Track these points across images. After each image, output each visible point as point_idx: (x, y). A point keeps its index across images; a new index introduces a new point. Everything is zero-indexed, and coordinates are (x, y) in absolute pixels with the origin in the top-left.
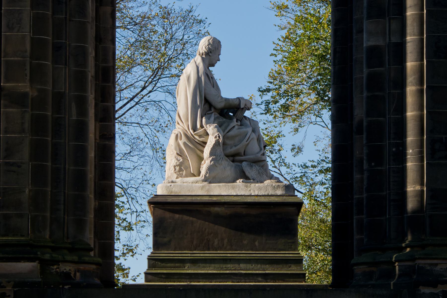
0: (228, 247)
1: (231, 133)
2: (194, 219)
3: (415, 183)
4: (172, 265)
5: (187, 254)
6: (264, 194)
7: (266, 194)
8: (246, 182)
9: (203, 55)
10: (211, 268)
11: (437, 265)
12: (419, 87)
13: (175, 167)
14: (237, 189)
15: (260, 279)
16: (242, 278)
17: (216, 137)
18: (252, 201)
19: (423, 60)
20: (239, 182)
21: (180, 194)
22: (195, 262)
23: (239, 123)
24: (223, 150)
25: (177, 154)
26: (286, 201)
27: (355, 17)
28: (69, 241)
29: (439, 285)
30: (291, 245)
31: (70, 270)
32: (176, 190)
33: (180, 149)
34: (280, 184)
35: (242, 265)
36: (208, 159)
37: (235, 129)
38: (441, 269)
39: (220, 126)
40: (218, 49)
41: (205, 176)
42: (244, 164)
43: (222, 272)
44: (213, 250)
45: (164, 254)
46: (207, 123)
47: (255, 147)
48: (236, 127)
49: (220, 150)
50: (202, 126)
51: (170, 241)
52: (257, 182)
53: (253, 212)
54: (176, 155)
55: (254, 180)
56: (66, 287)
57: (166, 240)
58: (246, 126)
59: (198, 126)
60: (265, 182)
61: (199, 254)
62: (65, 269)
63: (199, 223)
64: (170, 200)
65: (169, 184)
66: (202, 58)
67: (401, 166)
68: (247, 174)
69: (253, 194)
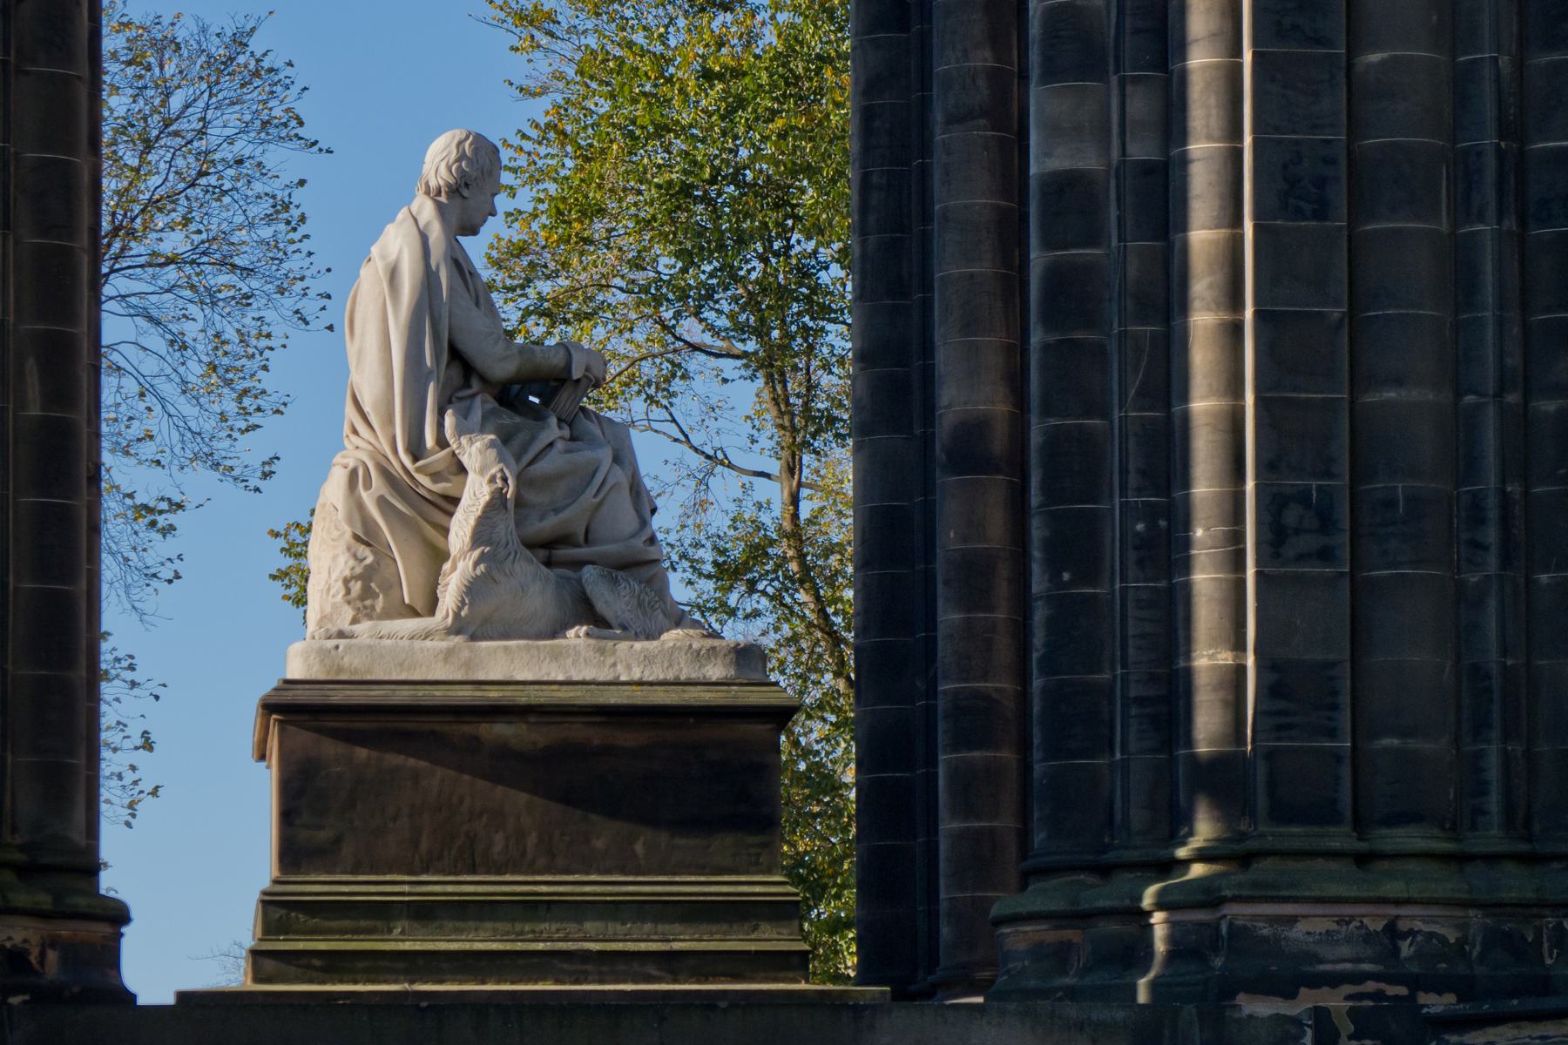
0: (542, 862)
1: (544, 466)
2: (423, 764)
3: (1214, 643)
5: (398, 886)
6: (661, 677)
7: (670, 676)
8: (599, 637)
9: (439, 193)
10: (482, 935)
11: (1292, 920)
12: (1226, 316)
13: (346, 581)
14: (569, 661)
15: (655, 973)
16: (589, 967)
17: (492, 480)
18: (625, 701)
19: (1237, 221)
21: (369, 677)
22: (424, 913)
24: (518, 524)
25: (357, 538)
26: (740, 702)
27: (939, 69)
28: (18, 841)
29: (1303, 990)
30: (759, 855)
31: (25, 941)
32: (354, 664)
33: (367, 522)
34: (716, 643)
35: (590, 927)
36: (463, 555)
37: (554, 452)
38: (1309, 933)
39: (506, 438)
40: (490, 173)
41: (457, 615)
42: (589, 573)
43: (519, 946)
44: (488, 873)
45: (318, 885)
46: (460, 431)
48: (560, 445)
49: (505, 526)
50: (442, 443)
51: (337, 841)
52: (637, 637)
53: (628, 738)
54: (353, 541)
55: (624, 628)
56: (15, 1000)
57: (324, 835)
58: (593, 443)
59: (430, 440)
60: (665, 636)
61: (439, 886)
62: (10, 938)
63: (438, 778)
64: (338, 696)
65: (331, 643)
66: (440, 207)
67: (1163, 584)
68: (600, 606)
69: (623, 678)
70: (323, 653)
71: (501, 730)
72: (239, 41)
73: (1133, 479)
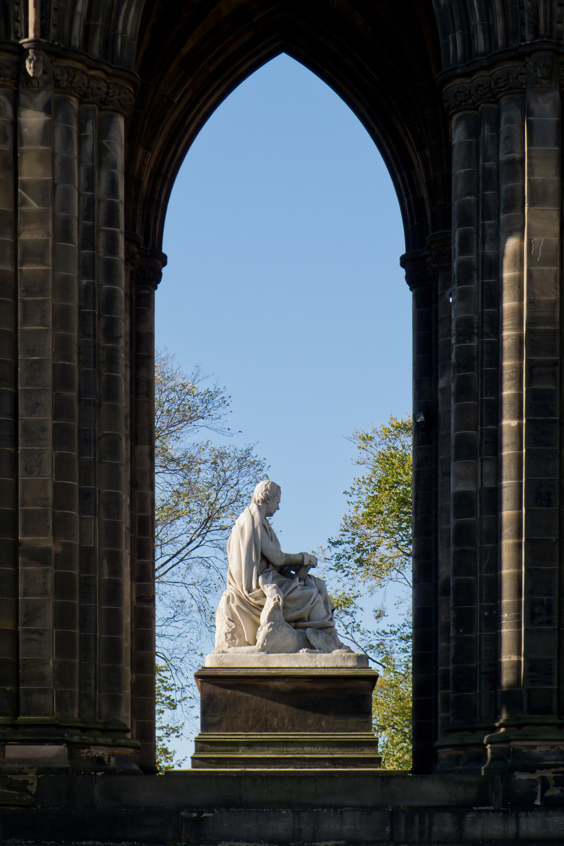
0: (290, 727)
1: (293, 595)
2: (250, 695)
3: (510, 653)
4: (223, 748)
5: (241, 736)
6: (332, 666)
7: (335, 665)
8: (311, 652)
9: (259, 502)
10: (269, 752)
11: (535, 747)
12: (516, 541)
13: (226, 634)
14: (300, 661)
15: (327, 764)
16: (306, 763)
17: (275, 600)
18: (318, 674)
19: (521, 508)
20: (303, 651)
21: (232, 666)
22: (250, 745)
23: (302, 583)
24: (284, 615)
25: (229, 619)
26: (357, 674)
28: (102, 721)
30: (364, 725)
31: (103, 754)
32: (227, 662)
33: (233, 614)
34: (350, 654)
35: (306, 749)
36: (265, 625)
37: (297, 590)
38: (540, 751)
39: (280, 586)
40: (277, 495)
41: (262, 645)
42: (309, 630)
43: (282, 756)
44: (272, 731)
45: (214, 736)
46: (264, 583)
47: (321, 611)
48: (299, 588)
49: (279, 615)
50: (258, 587)
51: (221, 721)
52: (324, 652)
53: (319, 686)
54: (228, 621)
55: (320, 649)
56: (99, 774)
57: (216, 719)
58: (311, 586)
59: (254, 586)
60: (333, 652)
61: (255, 736)
62: (97, 753)
63: (255, 700)
64: (220, 673)
65: (219, 655)
66: (259, 507)
67: (494, 633)
68: (312, 642)
69: (318, 666)
70: (217, 658)
71: (276, 684)
72: (248, 452)
73: (484, 598)
